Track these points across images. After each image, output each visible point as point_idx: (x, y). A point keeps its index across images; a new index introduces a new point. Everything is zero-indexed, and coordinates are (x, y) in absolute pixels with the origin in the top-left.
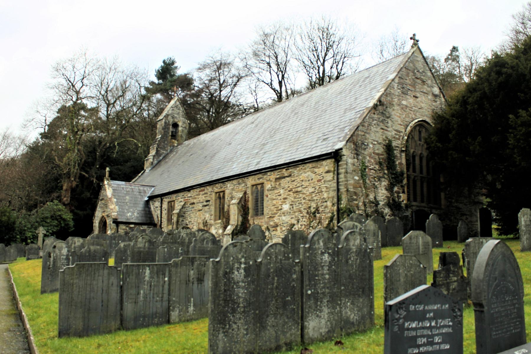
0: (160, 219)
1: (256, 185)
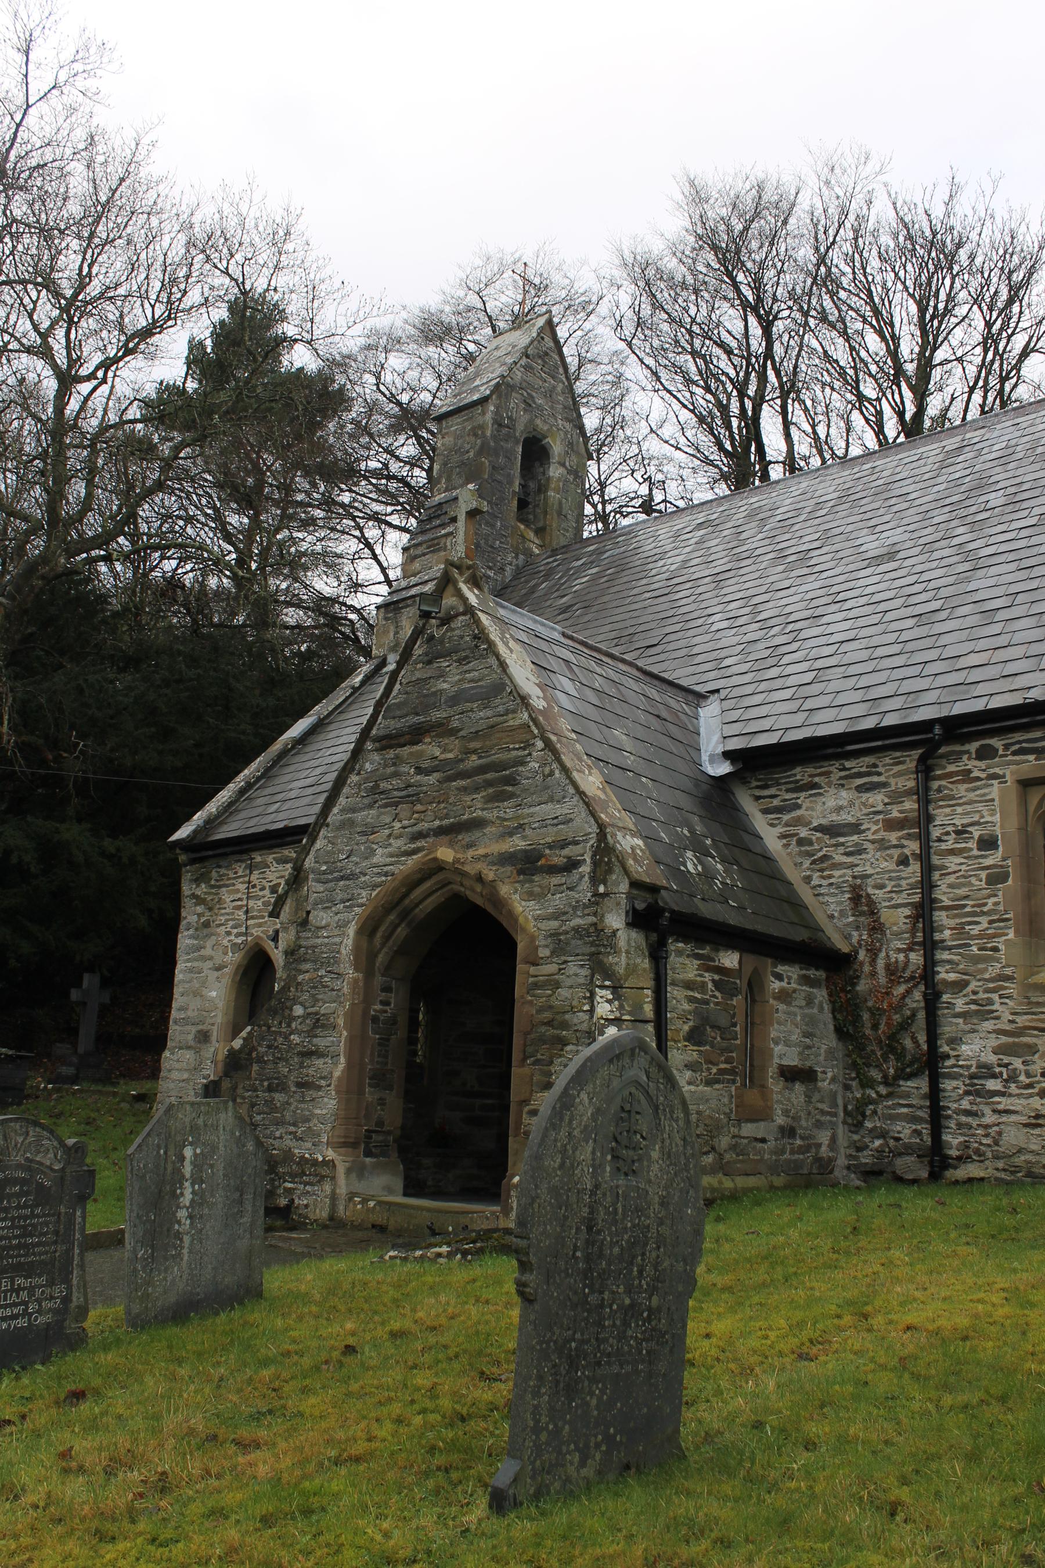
0: (897, 919)
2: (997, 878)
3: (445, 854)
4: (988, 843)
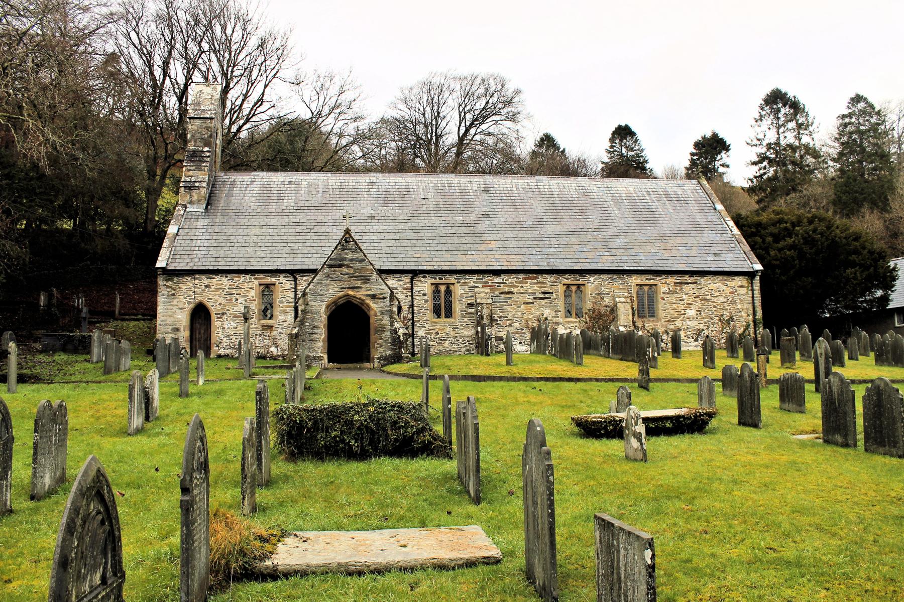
1: (641, 285)
2: (426, 301)
3: (351, 293)
4: (425, 295)
